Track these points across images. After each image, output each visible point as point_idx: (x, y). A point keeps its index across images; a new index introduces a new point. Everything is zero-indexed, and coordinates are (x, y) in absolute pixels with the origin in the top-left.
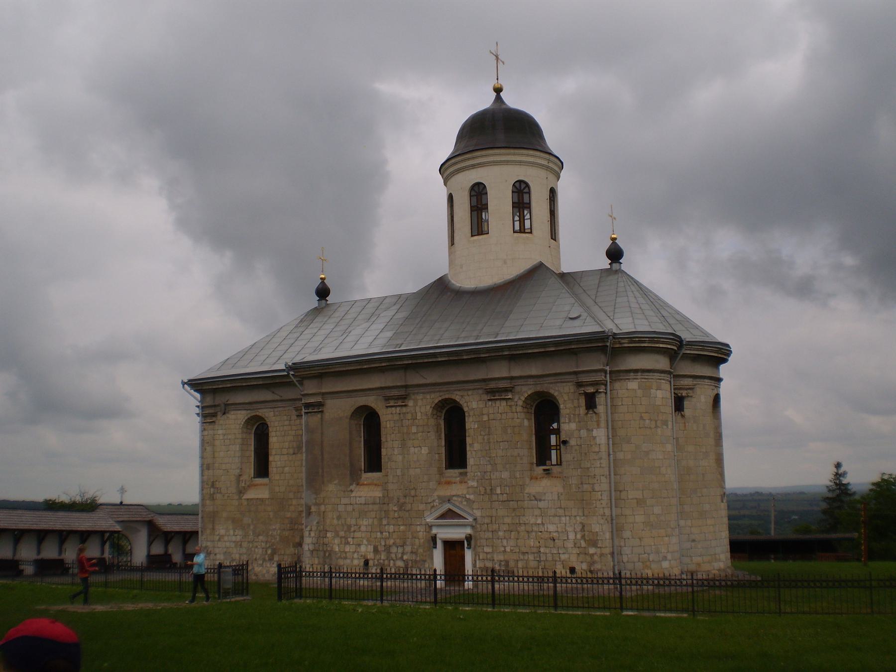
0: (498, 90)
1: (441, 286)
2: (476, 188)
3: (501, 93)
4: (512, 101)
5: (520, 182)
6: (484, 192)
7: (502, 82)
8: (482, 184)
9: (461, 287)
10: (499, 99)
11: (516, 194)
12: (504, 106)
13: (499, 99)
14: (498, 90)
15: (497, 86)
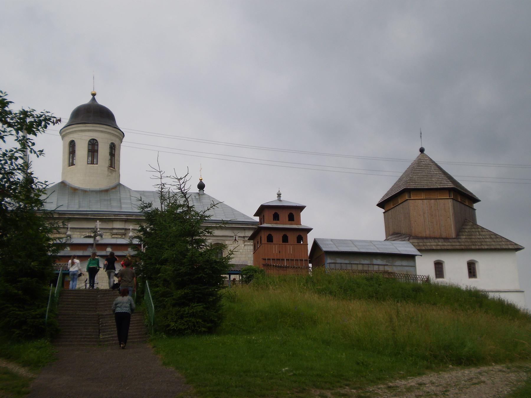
0: (94, 95)
1: (63, 184)
2: (92, 141)
3: (95, 96)
4: (101, 101)
5: (112, 143)
6: (97, 144)
7: (96, 91)
8: (97, 140)
9: (110, 186)
10: (94, 99)
11: (91, 146)
12: (96, 103)
13: (94, 99)
14: (94, 95)
15: (94, 92)
